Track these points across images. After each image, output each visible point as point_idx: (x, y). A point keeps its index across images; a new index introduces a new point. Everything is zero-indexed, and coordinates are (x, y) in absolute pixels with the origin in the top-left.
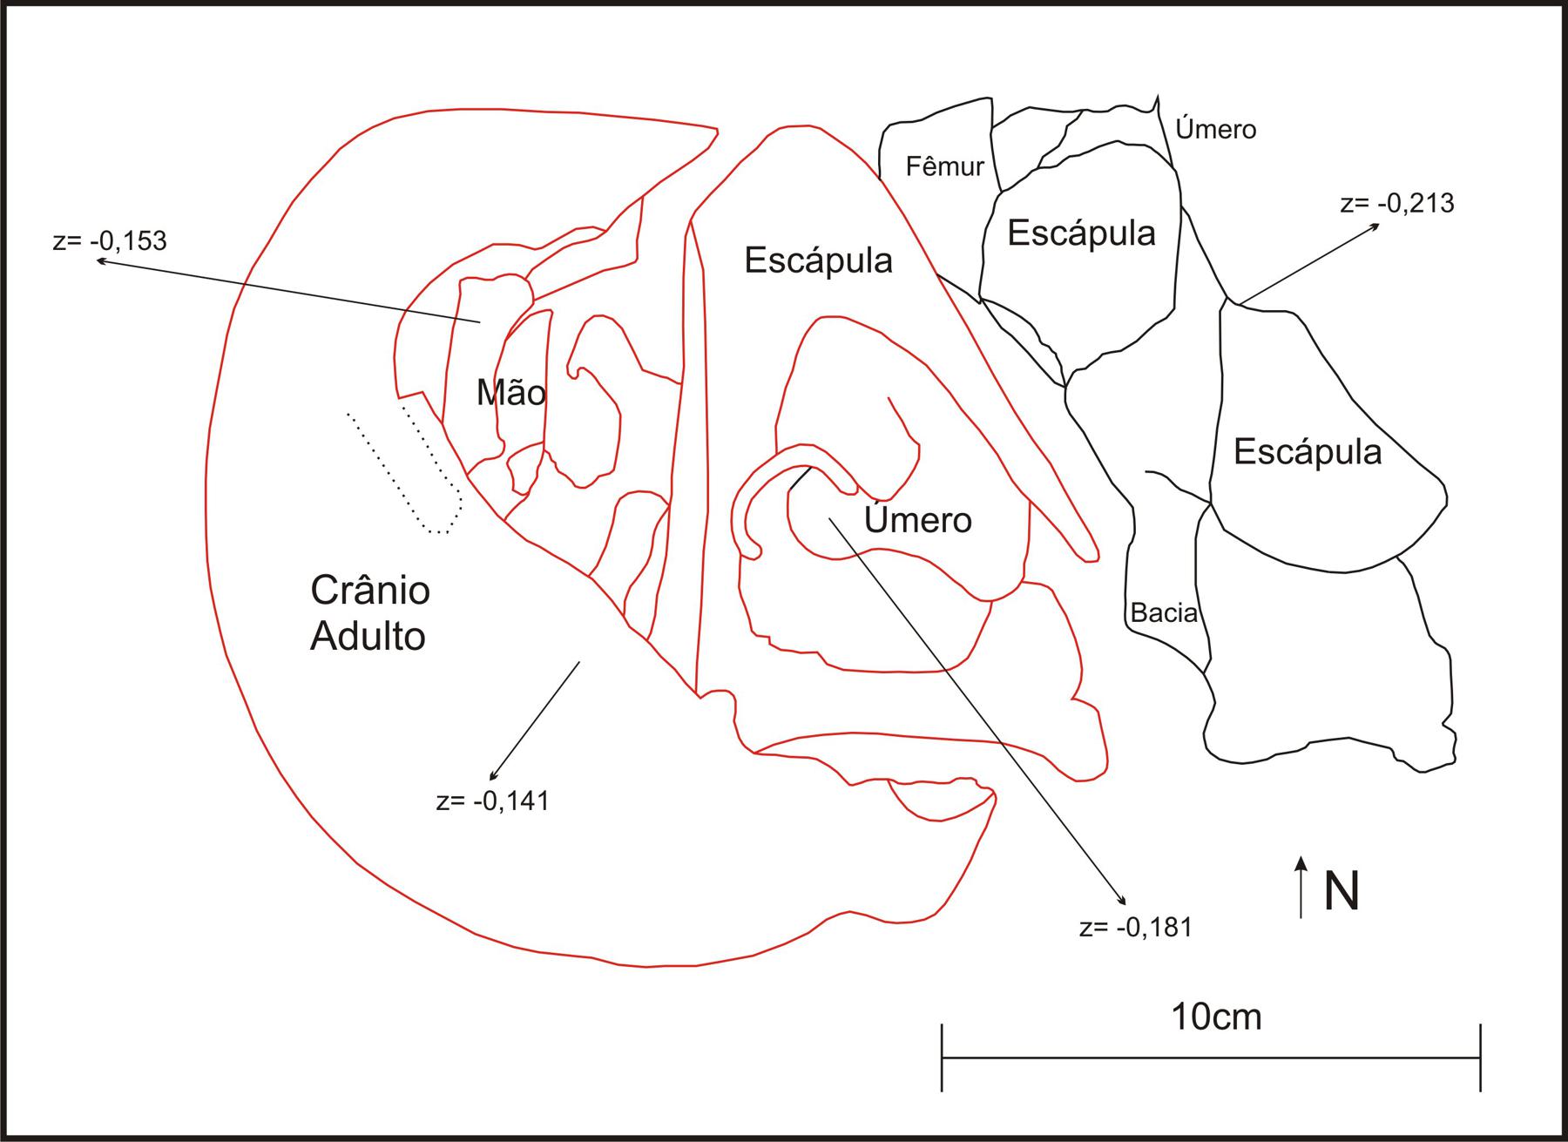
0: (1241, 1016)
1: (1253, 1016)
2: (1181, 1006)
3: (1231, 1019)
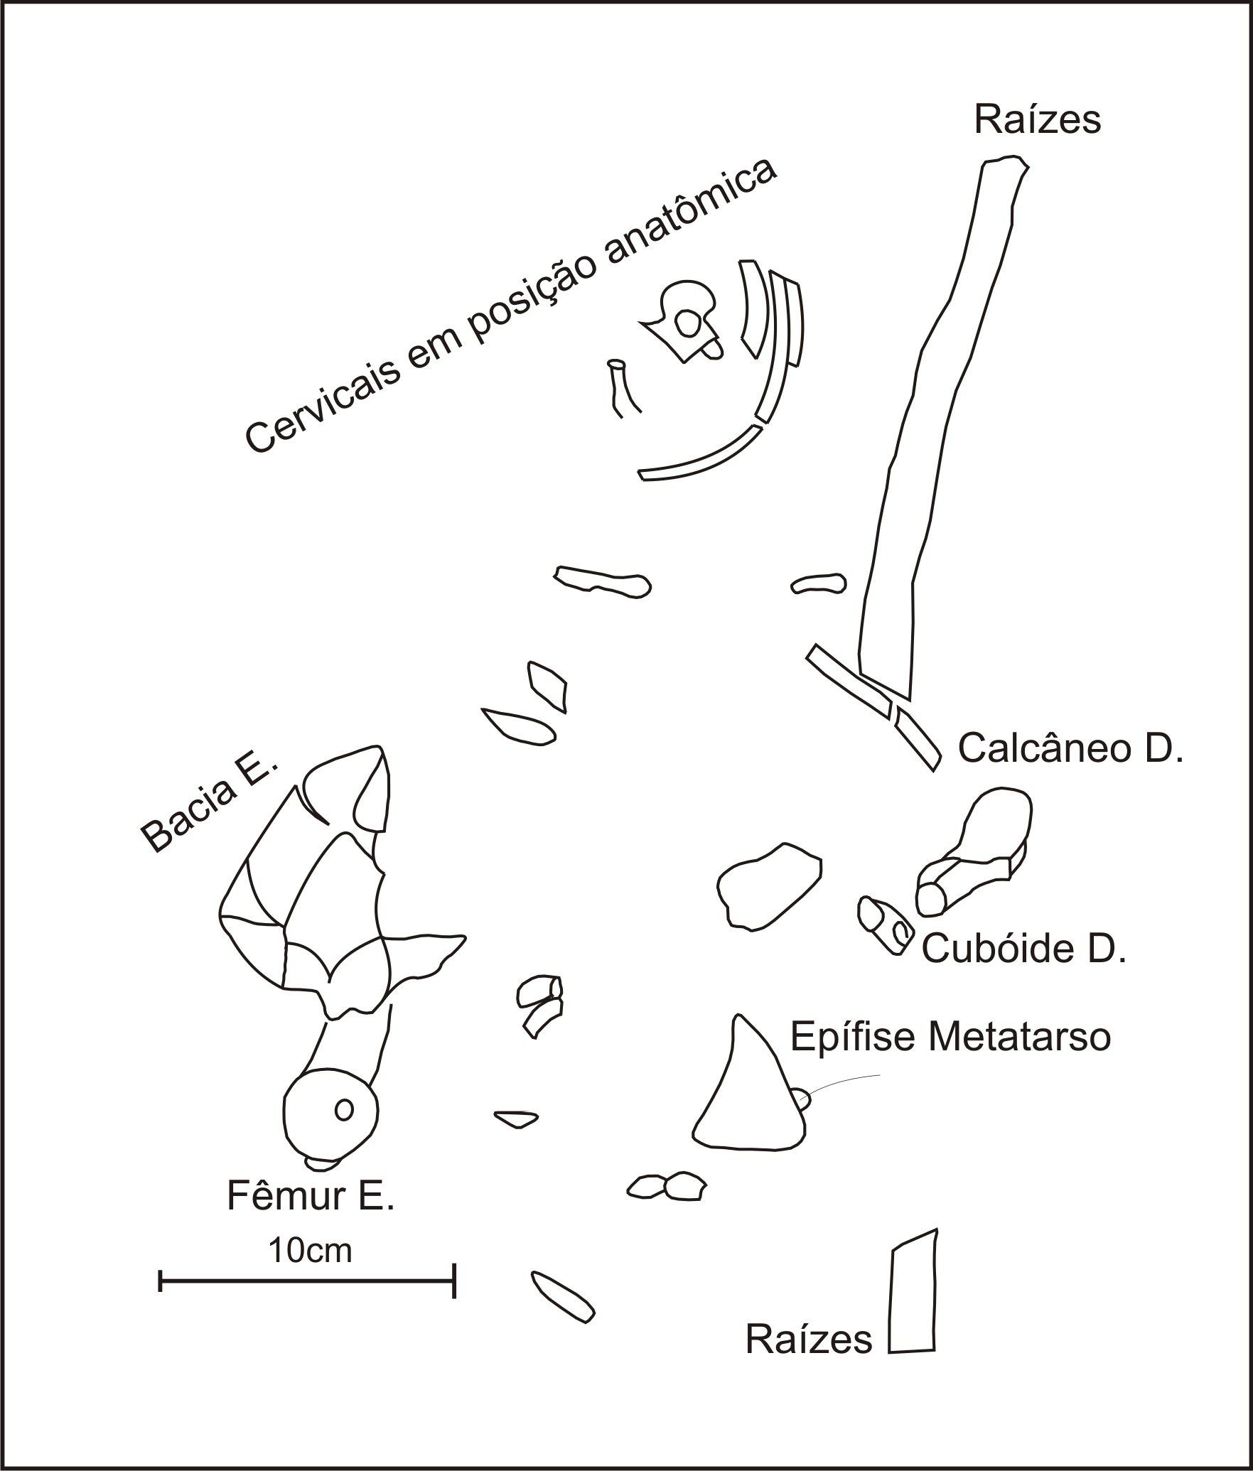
0: (333, 1250)
1: (344, 1250)
2: (277, 1241)
3: (323, 1252)
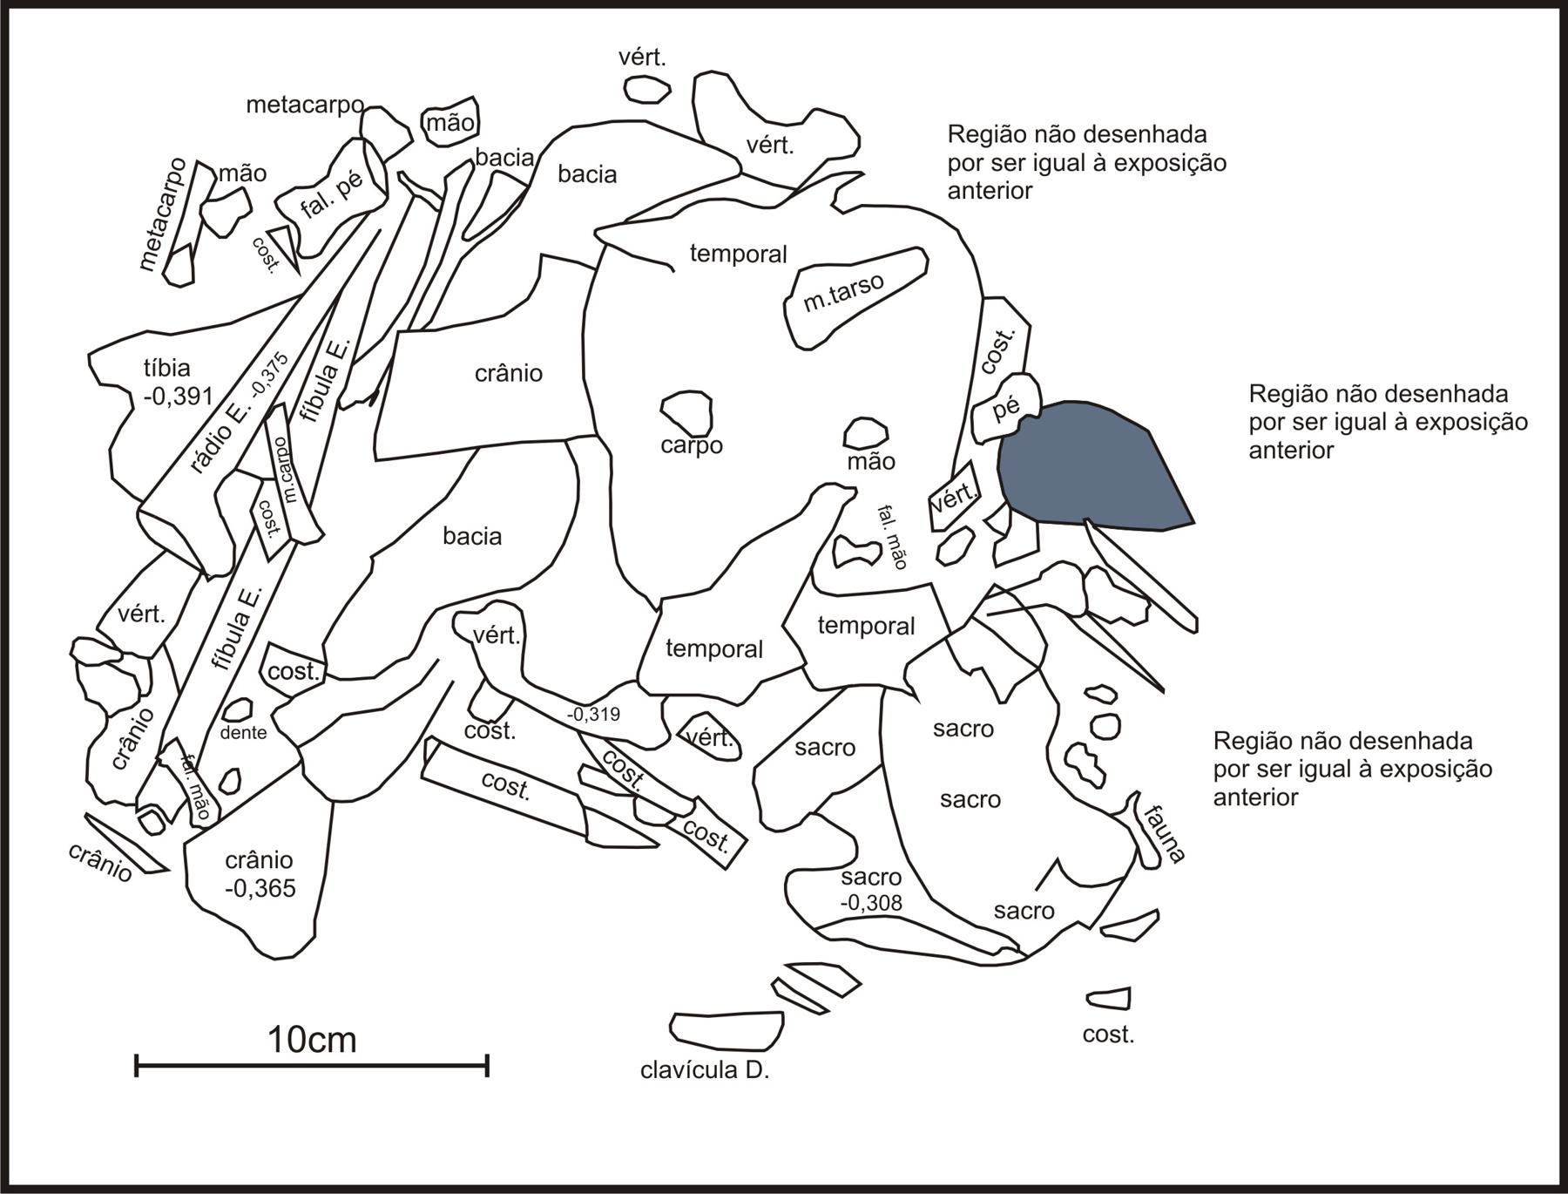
0: (336, 1039)
1: (348, 1040)
2: (277, 1029)
3: (326, 1042)
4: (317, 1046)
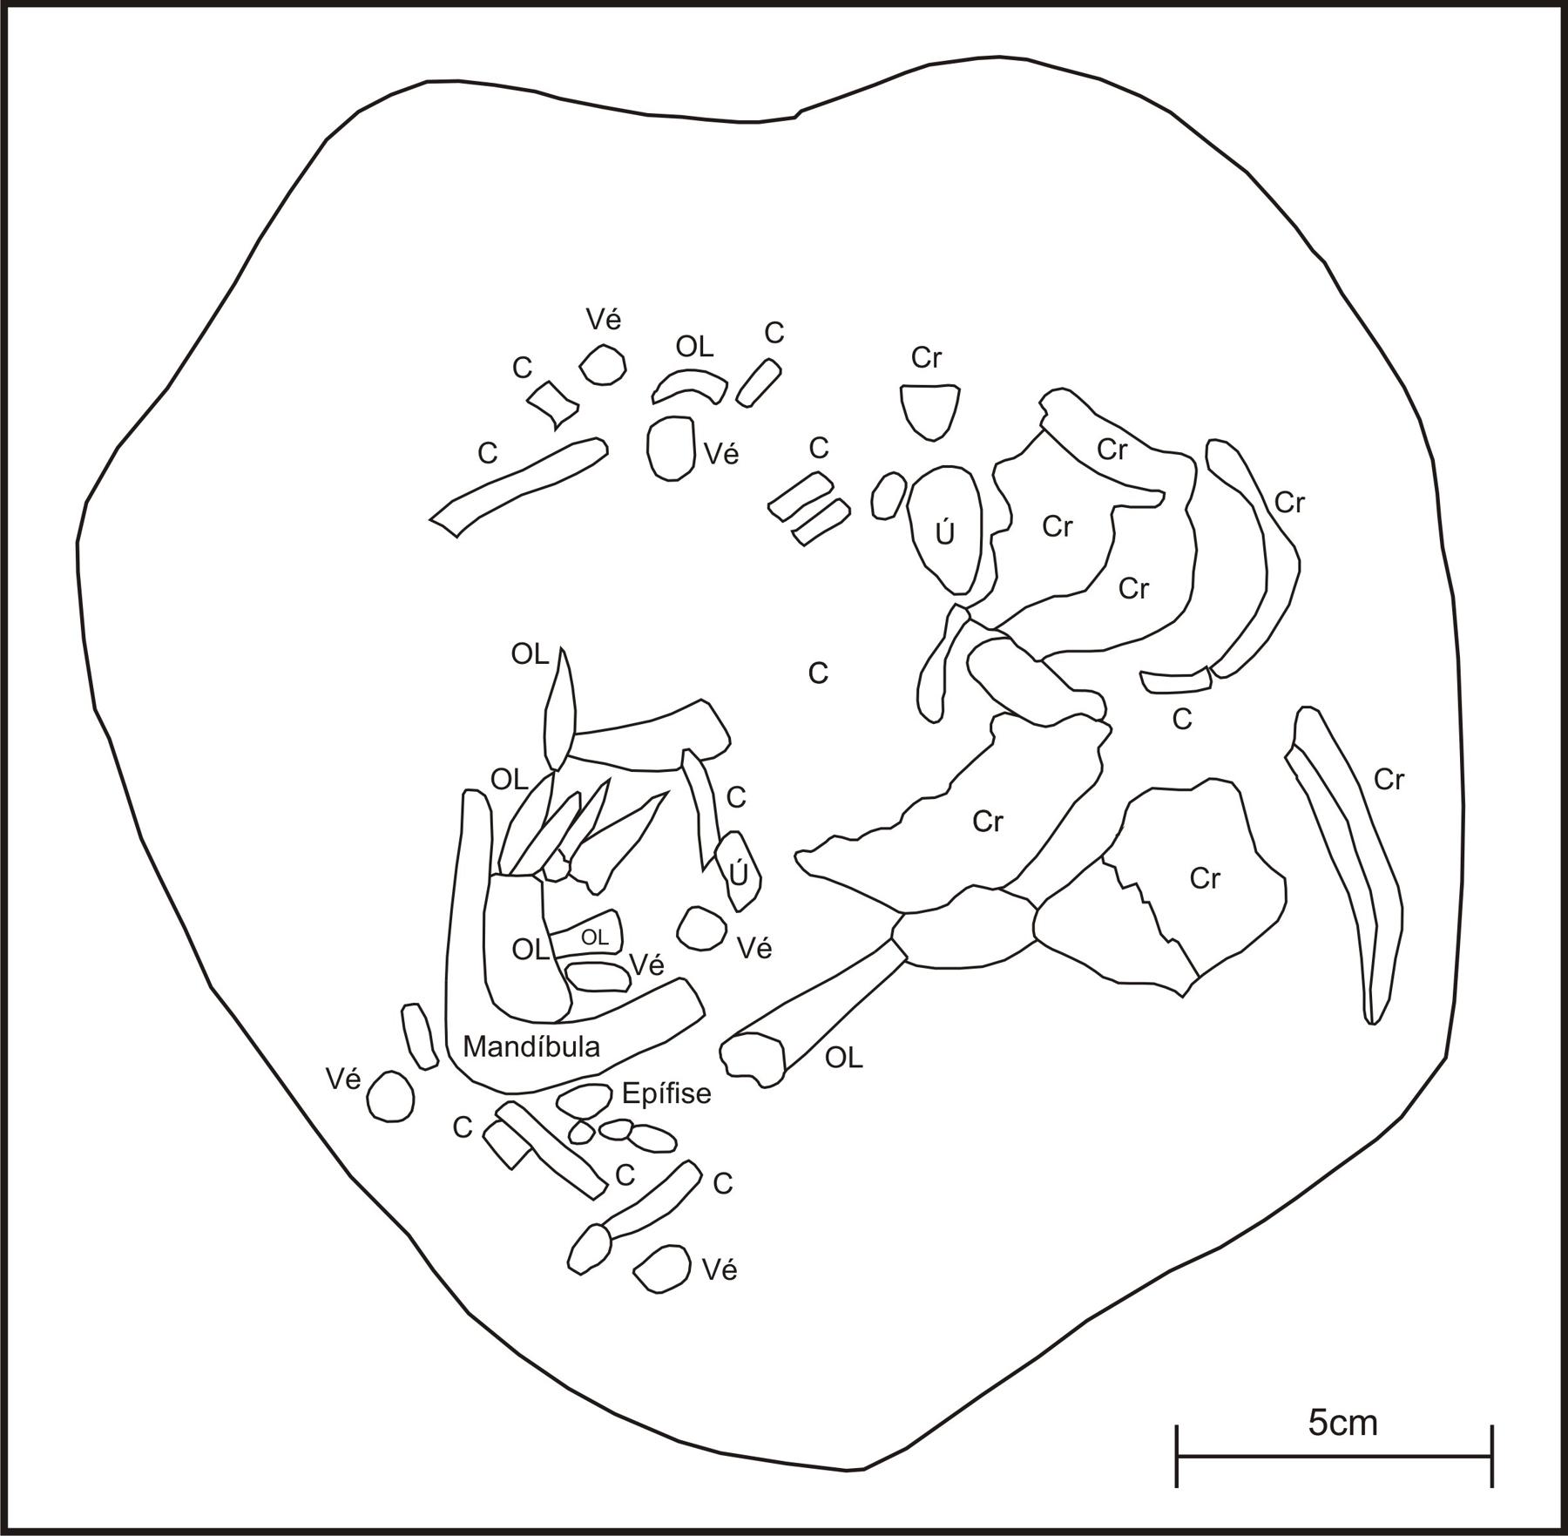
0: (1358, 1422)
1: (1369, 1422)
3: (1347, 1425)
4: (1338, 1429)
